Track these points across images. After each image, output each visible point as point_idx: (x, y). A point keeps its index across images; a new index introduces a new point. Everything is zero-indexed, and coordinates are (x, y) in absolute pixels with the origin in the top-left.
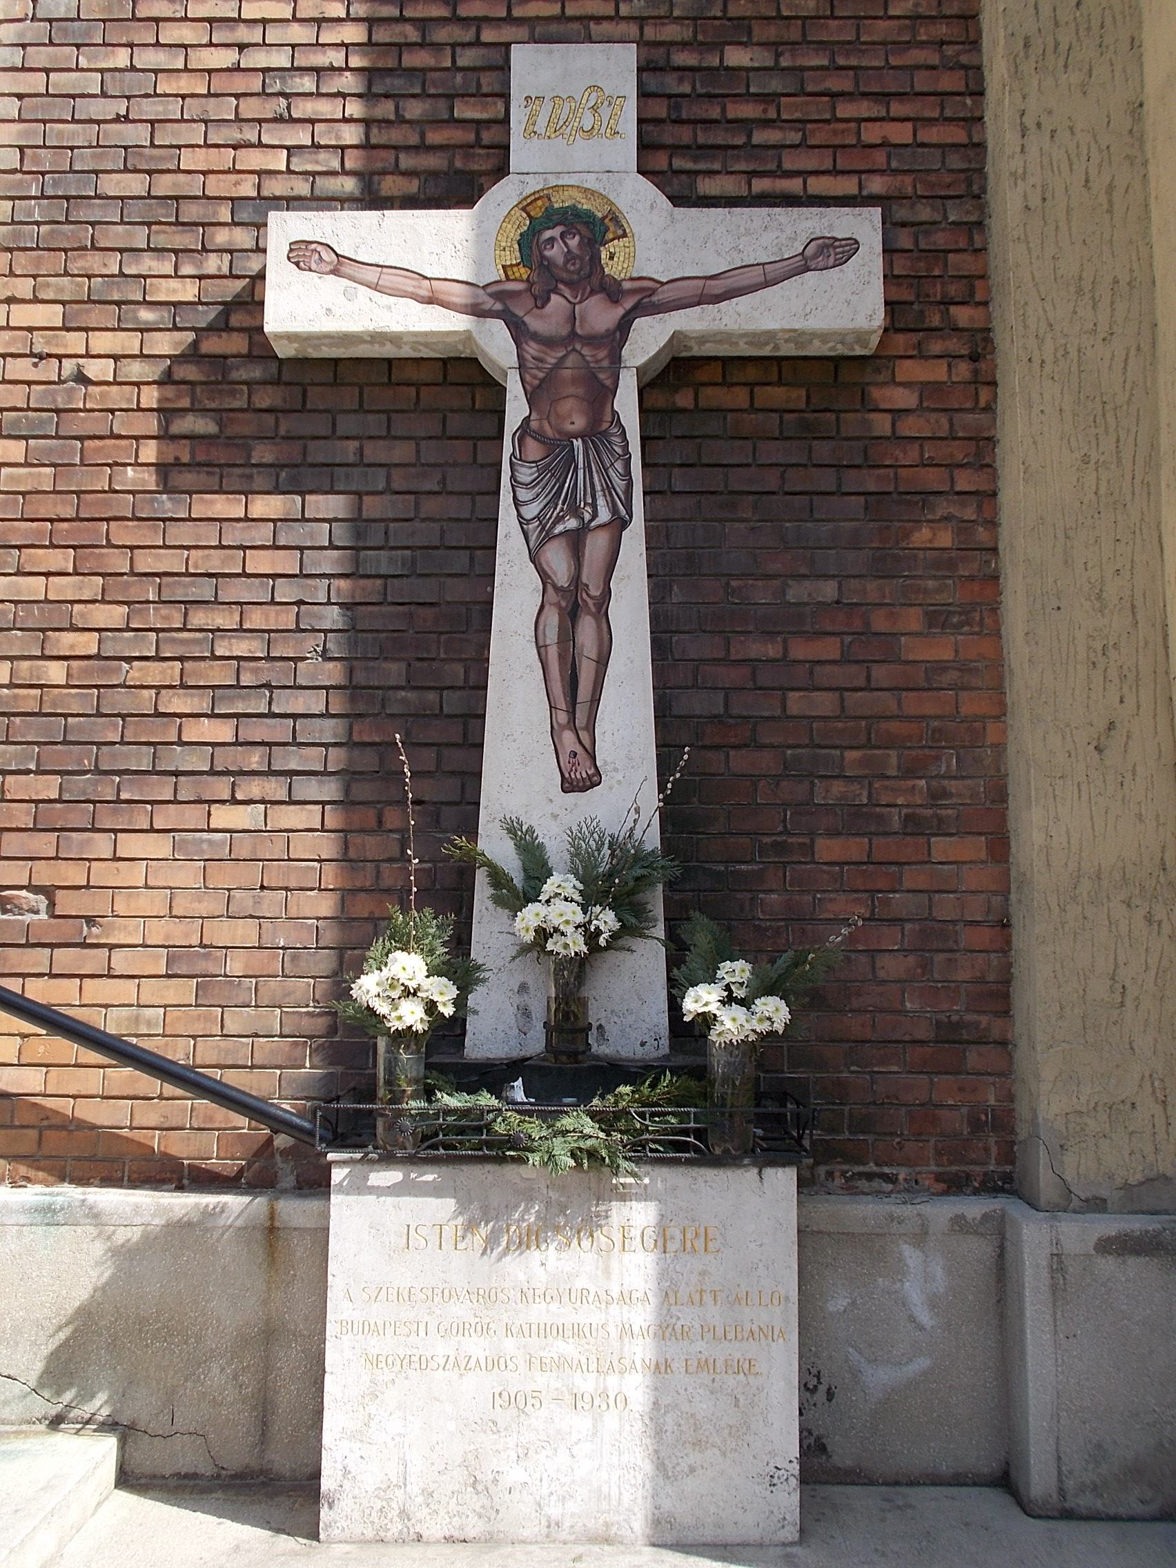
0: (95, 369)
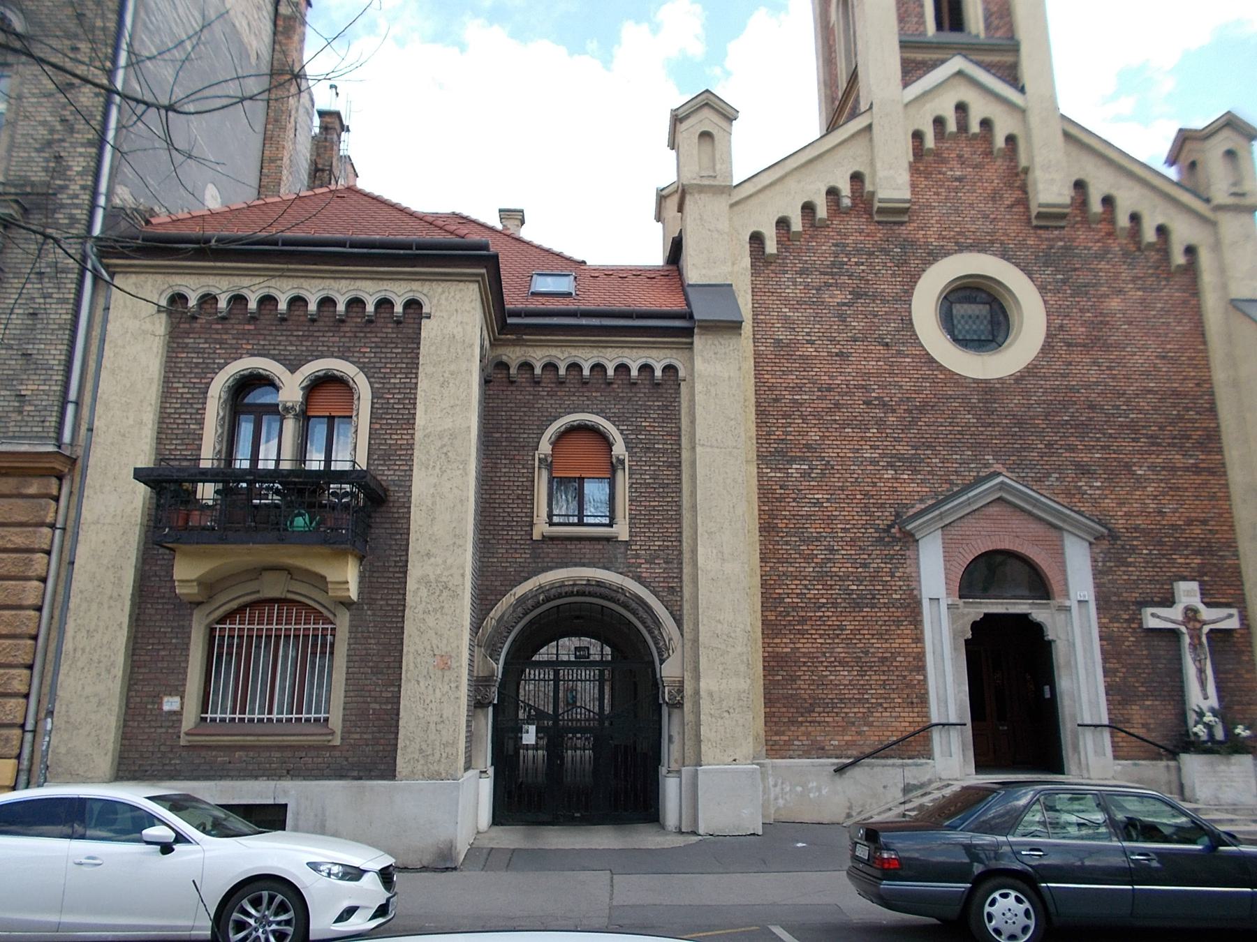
0: (1115, 629)
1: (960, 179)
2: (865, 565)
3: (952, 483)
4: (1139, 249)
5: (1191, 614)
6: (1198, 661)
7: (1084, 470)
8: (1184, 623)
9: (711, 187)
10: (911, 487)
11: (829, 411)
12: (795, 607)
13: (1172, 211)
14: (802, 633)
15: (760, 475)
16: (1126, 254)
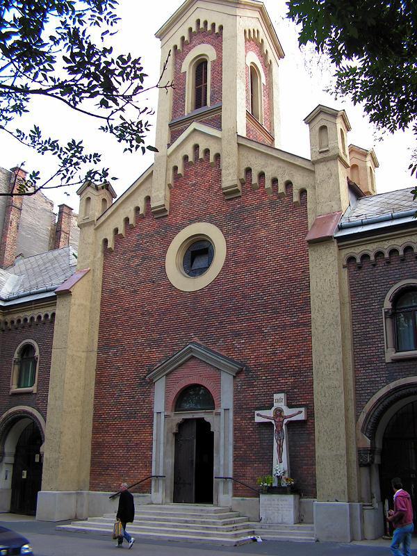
1: (194, 185)
2: (133, 397)
3: (173, 350)
4: (279, 198)
5: (279, 412)
6: (280, 440)
7: (237, 334)
8: (274, 419)
9: (87, 223)
10: (157, 355)
11: (127, 321)
12: (105, 419)
13: (294, 171)
14: (107, 432)
15: (98, 357)
16: (272, 202)
